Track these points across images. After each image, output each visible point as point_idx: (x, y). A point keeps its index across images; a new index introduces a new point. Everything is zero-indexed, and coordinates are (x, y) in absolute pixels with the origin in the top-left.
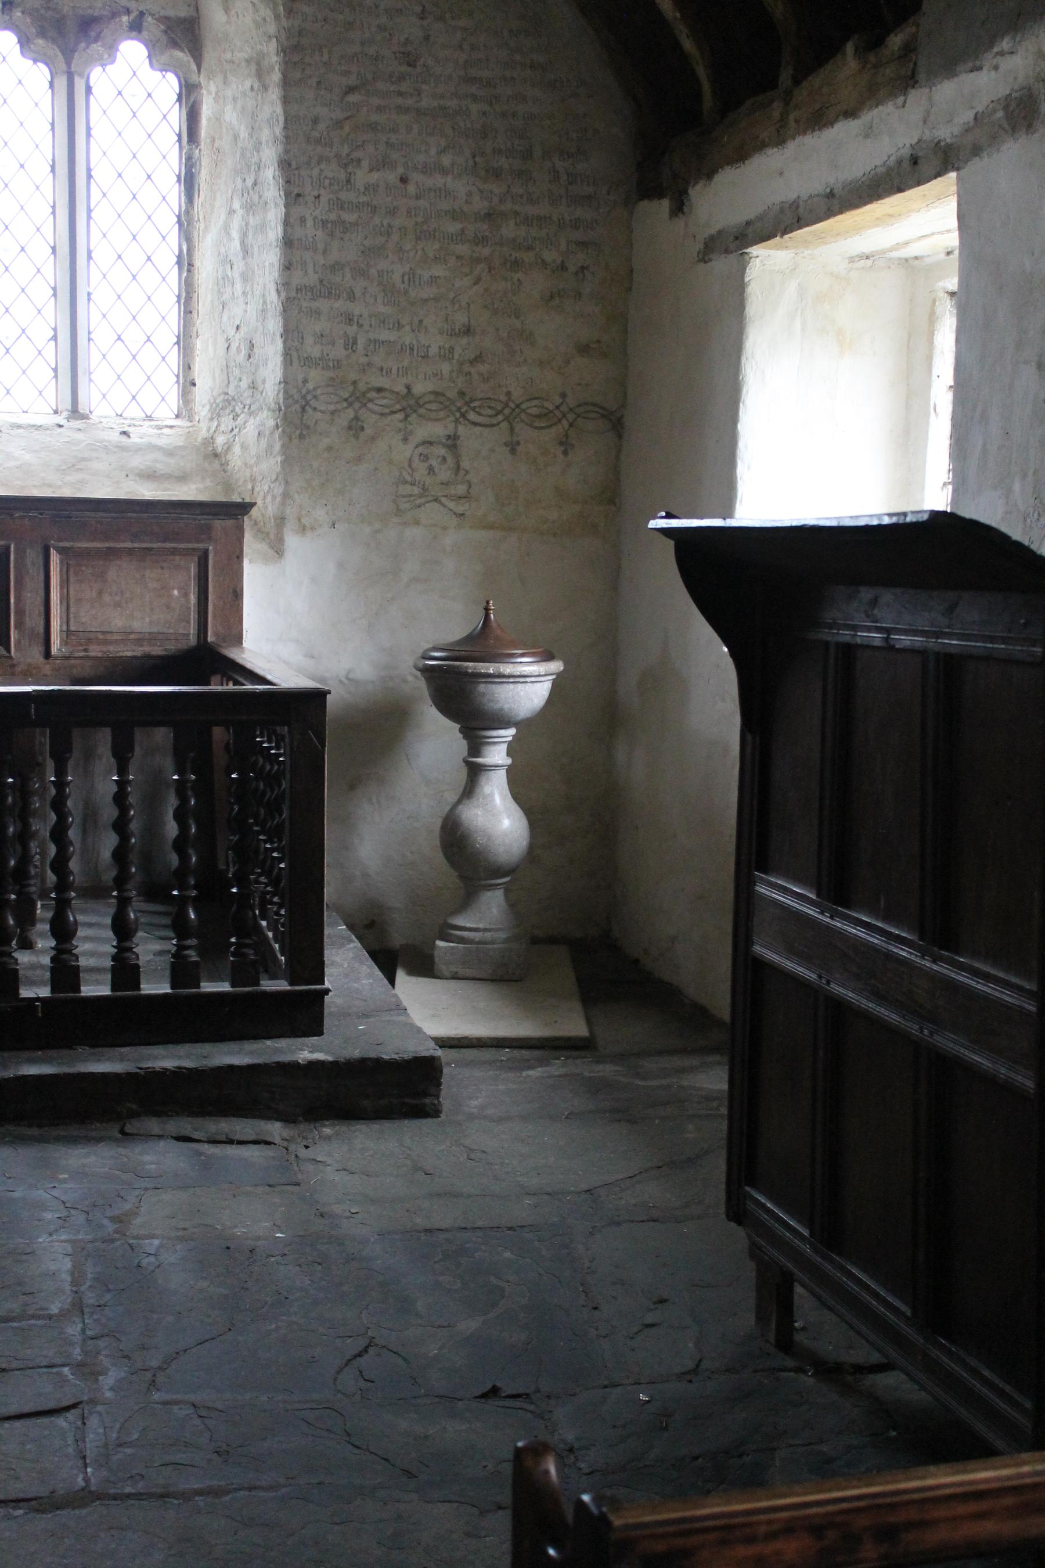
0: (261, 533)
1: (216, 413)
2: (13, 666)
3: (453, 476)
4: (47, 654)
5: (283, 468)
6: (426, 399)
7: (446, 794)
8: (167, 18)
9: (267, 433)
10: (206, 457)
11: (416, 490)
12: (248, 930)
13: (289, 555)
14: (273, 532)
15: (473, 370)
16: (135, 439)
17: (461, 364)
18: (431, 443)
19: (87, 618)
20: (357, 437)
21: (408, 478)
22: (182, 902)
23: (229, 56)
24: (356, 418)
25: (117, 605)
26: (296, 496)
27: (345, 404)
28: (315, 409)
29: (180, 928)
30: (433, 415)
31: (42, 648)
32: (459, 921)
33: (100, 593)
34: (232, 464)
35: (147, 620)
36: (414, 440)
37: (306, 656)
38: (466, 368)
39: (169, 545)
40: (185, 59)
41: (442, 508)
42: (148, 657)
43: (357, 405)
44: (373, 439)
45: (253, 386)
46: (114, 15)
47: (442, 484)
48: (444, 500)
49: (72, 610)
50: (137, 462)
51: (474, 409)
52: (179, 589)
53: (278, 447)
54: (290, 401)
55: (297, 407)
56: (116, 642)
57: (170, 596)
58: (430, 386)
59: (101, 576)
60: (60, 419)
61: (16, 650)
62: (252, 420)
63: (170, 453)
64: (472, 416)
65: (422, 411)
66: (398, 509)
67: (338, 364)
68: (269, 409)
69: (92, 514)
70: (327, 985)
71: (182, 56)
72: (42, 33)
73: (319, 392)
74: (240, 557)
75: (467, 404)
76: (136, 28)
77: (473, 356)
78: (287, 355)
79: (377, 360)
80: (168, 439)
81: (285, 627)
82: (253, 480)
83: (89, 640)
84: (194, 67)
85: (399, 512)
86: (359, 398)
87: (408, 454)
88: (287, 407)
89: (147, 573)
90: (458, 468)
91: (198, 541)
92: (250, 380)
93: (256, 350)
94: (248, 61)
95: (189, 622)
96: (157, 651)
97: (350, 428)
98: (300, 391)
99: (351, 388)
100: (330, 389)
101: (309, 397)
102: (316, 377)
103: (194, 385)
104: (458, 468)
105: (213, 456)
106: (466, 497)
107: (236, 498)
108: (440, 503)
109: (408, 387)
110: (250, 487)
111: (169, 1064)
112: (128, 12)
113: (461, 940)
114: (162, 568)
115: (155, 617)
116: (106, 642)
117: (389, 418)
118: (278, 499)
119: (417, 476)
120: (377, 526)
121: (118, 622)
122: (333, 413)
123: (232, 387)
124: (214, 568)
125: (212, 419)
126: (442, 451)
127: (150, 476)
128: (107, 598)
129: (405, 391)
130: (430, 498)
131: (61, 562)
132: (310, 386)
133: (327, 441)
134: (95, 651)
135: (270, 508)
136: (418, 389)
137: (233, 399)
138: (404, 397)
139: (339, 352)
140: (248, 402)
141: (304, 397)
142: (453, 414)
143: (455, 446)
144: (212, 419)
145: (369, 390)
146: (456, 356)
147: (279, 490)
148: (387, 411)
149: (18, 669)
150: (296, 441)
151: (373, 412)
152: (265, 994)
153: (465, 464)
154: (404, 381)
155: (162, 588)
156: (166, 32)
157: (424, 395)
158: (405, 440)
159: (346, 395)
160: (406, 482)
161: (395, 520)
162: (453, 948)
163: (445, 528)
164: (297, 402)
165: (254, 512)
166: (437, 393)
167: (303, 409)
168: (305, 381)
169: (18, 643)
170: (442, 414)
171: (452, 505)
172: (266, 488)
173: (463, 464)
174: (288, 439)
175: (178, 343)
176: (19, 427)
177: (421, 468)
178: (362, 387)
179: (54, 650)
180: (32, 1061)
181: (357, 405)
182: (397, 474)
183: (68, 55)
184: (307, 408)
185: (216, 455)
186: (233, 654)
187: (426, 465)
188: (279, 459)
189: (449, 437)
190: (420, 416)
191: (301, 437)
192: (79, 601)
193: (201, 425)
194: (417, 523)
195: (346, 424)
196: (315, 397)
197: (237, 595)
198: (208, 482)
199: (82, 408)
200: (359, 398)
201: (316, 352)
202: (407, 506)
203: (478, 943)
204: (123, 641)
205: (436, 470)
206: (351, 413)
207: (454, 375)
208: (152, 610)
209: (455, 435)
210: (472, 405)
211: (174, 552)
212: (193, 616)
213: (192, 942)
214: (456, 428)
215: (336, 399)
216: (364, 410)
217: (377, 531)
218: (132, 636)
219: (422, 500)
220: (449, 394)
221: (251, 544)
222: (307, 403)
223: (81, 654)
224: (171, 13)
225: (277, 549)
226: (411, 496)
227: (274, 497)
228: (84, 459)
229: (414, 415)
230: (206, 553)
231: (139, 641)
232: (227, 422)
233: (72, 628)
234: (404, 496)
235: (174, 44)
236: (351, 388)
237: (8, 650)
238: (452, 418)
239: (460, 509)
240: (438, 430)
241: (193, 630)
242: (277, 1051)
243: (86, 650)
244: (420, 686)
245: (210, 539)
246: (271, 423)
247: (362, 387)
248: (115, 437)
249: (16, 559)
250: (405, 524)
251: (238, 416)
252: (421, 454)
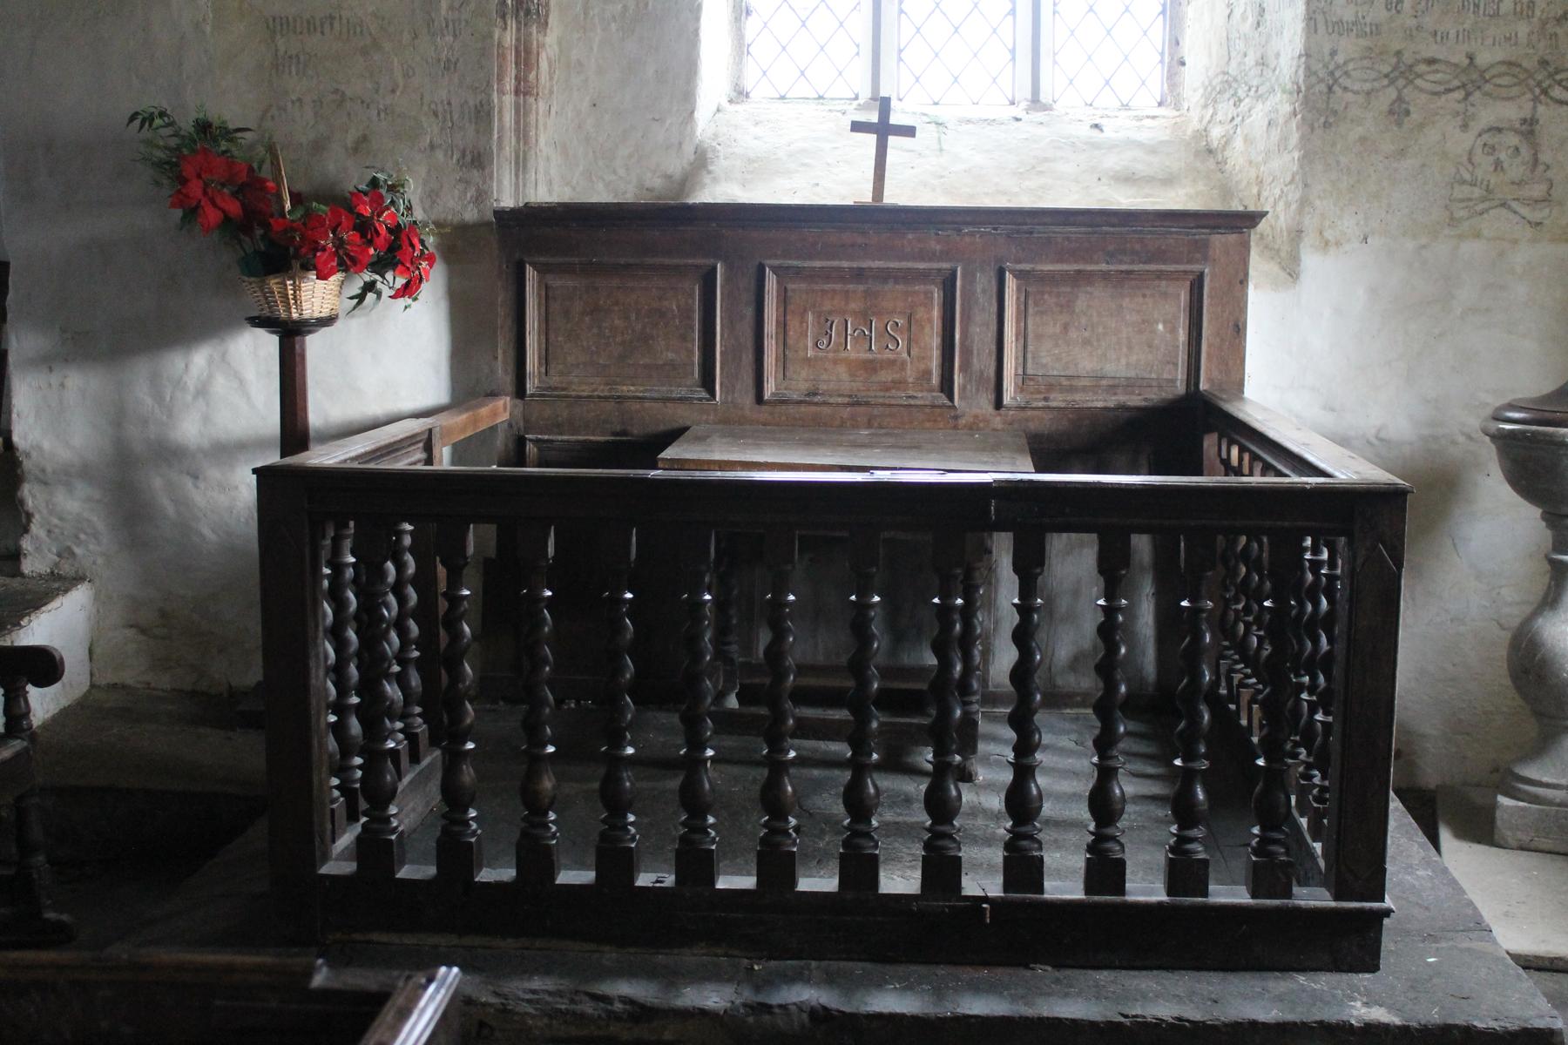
0: (1271, 251)
1: (1211, 99)
2: (956, 418)
4: (998, 404)
5: (1301, 167)
6: (1494, 71)
7: (1504, 591)
9: (1281, 121)
10: (1197, 154)
11: (1477, 192)
12: (1274, 818)
13: (1306, 278)
14: (1286, 248)
15: (1559, 31)
16: (1109, 133)
17: (1544, 23)
18: (1499, 130)
19: (1052, 359)
20: (1399, 124)
21: (1467, 176)
22: (1187, 777)
24: (1400, 99)
25: (1087, 342)
26: (1318, 203)
27: (1386, 82)
28: (1345, 89)
29: (1184, 812)
30: (1504, 92)
31: (992, 397)
32: (1530, 771)
33: (1066, 327)
34: (1231, 162)
35: (1123, 361)
36: (1476, 126)
37: (1324, 408)
38: (1550, 28)
39: (1153, 267)
41: (1511, 216)
42: (1124, 408)
43: (1401, 82)
44: (1421, 126)
45: (1262, 63)
48: (1515, 205)
49: (1030, 348)
50: (1112, 162)
51: (1559, 83)
52: (1165, 323)
53: (1295, 138)
54: (1313, 79)
55: (1323, 87)
56: (1084, 389)
57: (1154, 331)
58: (1500, 54)
59: (1068, 307)
60: (1018, 111)
61: (960, 398)
62: (1260, 106)
63: (1152, 150)
64: (1557, 92)
65: (1488, 87)
66: (1452, 219)
67: (1376, 29)
68: (1284, 91)
69: (1058, 229)
70: (1388, 902)
73: (1351, 66)
74: (1244, 282)
75: (1551, 76)
77: (1560, 12)
78: (1311, 20)
79: (1429, 21)
80: (1153, 132)
81: (1314, 377)
82: (1260, 182)
83: (1050, 387)
85: (1453, 221)
86: (1403, 72)
87: (1467, 145)
88: (1308, 88)
89: (1126, 302)
90: (1536, 162)
91: (1189, 262)
92: (1259, 55)
93: (1267, 16)
95: (1176, 365)
96: (1135, 401)
97: (1391, 112)
98: (1326, 66)
99: (1394, 60)
100: (1366, 63)
101: (1337, 74)
102: (1348, 47)
103: (1183, 64)
104: (1536, 162)
105: (1208, 153)
106: (1546, 200)
107: (1236, 206)
108: (1509, 208)
109: (1471, 58)
110: (1255, 190)
111: (1165, 1011)
113: (1535, 799)
114: (1144, 296)
115: (1134, 358)
116: (1072, 389)
117: (1443, 98)
118: (1294, 207)
119: (1479, 173)
120: (1424, 241)
121: (1086, 363)
122: (1368, 93)
123: (1234, 64)
124: (1211, 297)
125: (1205, 106)
126: (1513, 140)
127: (1127, 179)
128: (1073, 334)
129: (1467, 61)
130: (1497, 202)
131: (1019, 289)
132: (1340, 59)
133: (1360, 130)
134: (1058, 400)
135: (1282, 218)
136: (1484, 58)
137: (1235, 80)
138: (1464, 71)
139: (1378, 13)
140: (1255, 83)
141: (1332, 73)
142: (1531, 90)
143: (1532, 132)
144: (1205, 106)
145: (1418, 62)
146: (1538, 13)
147: (1294, 195)
148: (1441, 88)
149: (962, 422)
150: (1319, 132)
151: (1422, 90)
152: (1298, 909)
153: (1545, 157)
154: (1466, 48)
155: (1144, 322)
157: (1492, 66)
158: (1465, 127)
159: (1386, 69)
160: (1464, 182)
161: (1447, 231)
162: (1522, 809)
163: (1515, 242)
164: (1321, 81)
165: (1263, 226)
166: (1510, 64)
167: (1330, 88)
168: (1333, 53)
169: (963, 389)
170: (1515, 91)
171: (1525, 211)
172: (1277, 192)
173: (1543, 157)
174: (1309, 127)
175: (1163, 12)
176: (969, 121)
177: (1485, 163)
178: (1408, 58)
179: (1007, 399)
180: (976, 988)
181: (1401, 82)
182: (1453, 170)
184: (1336, 88)
185: (1210, 151)
186: (1233, 408)
187: (1491, 158)
188: (1296, 155)
189: (1524, 121)
191: (1327, 125)
192: (1039, 337)
193: (1192, 113)
194: (1478, 235)
195: (1385, 108)
196: (1346, 73)
197: (1239, 330)
198: (1201, 187)
199: (1044, 97)
200: (1403, 72)
201: (1348, 15)
202: (1462, 213)
203: (1559, 805)
204: (1094, 388)
205: (1505, 165)
206: (1392, 93)
207: (1534, 38)
208: (1130, 348)
210: (1558, 77)
211: (1160, 275)
212: (1182, 358)
213: (1197, 832)
214: (1535, 108)
215: (1373, 75)
216: (1410, 88)
217: (1424, 247)
218: (1104, 382)
219: (1487, 205)
220: (1525, 64)
221: (1259, 266)
222: (1336, 81)
223: (1040, 404)
225: (1291, 270)
226: (1470, 199)
227: (1288, 205)
228: (1046, 160)
229: (1477, 94)
230: (1201, 276)
231: (1112, 389)
232: (1225, 109)
233: (1030, 371)
234: (1462, 201)
236: (1394, 60)
237: (951, 398)
238: (1529, 96)
239: (1536, 216)
240: (1511, 112)
241: (1181, 375)
242: (1316, 997)
243: (1046, 399)
244: (1489, 454)
245: (1205, 259)
246: (1287, 108)
247: (1408, 58)
248: (1085, 131)
249: (963, 286)
250: (1461, 237)
251: (1240, 101)
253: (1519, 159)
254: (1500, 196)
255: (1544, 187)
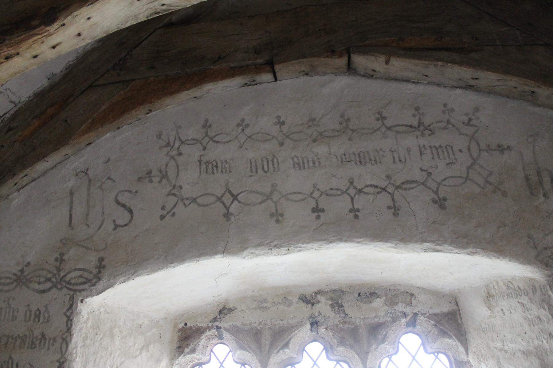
8: (435, 315)
23: (499, 345)
40: (454, 343)
46: (395, 320)
71: (452, 342)
72: (342, 342)
76: (412, 324)
84: (462, 349)
94: (526, 354)
112: (405, 315)
156: (436, 325)
183: (364, 356)
224: (437, 310)
235: (444, 333)
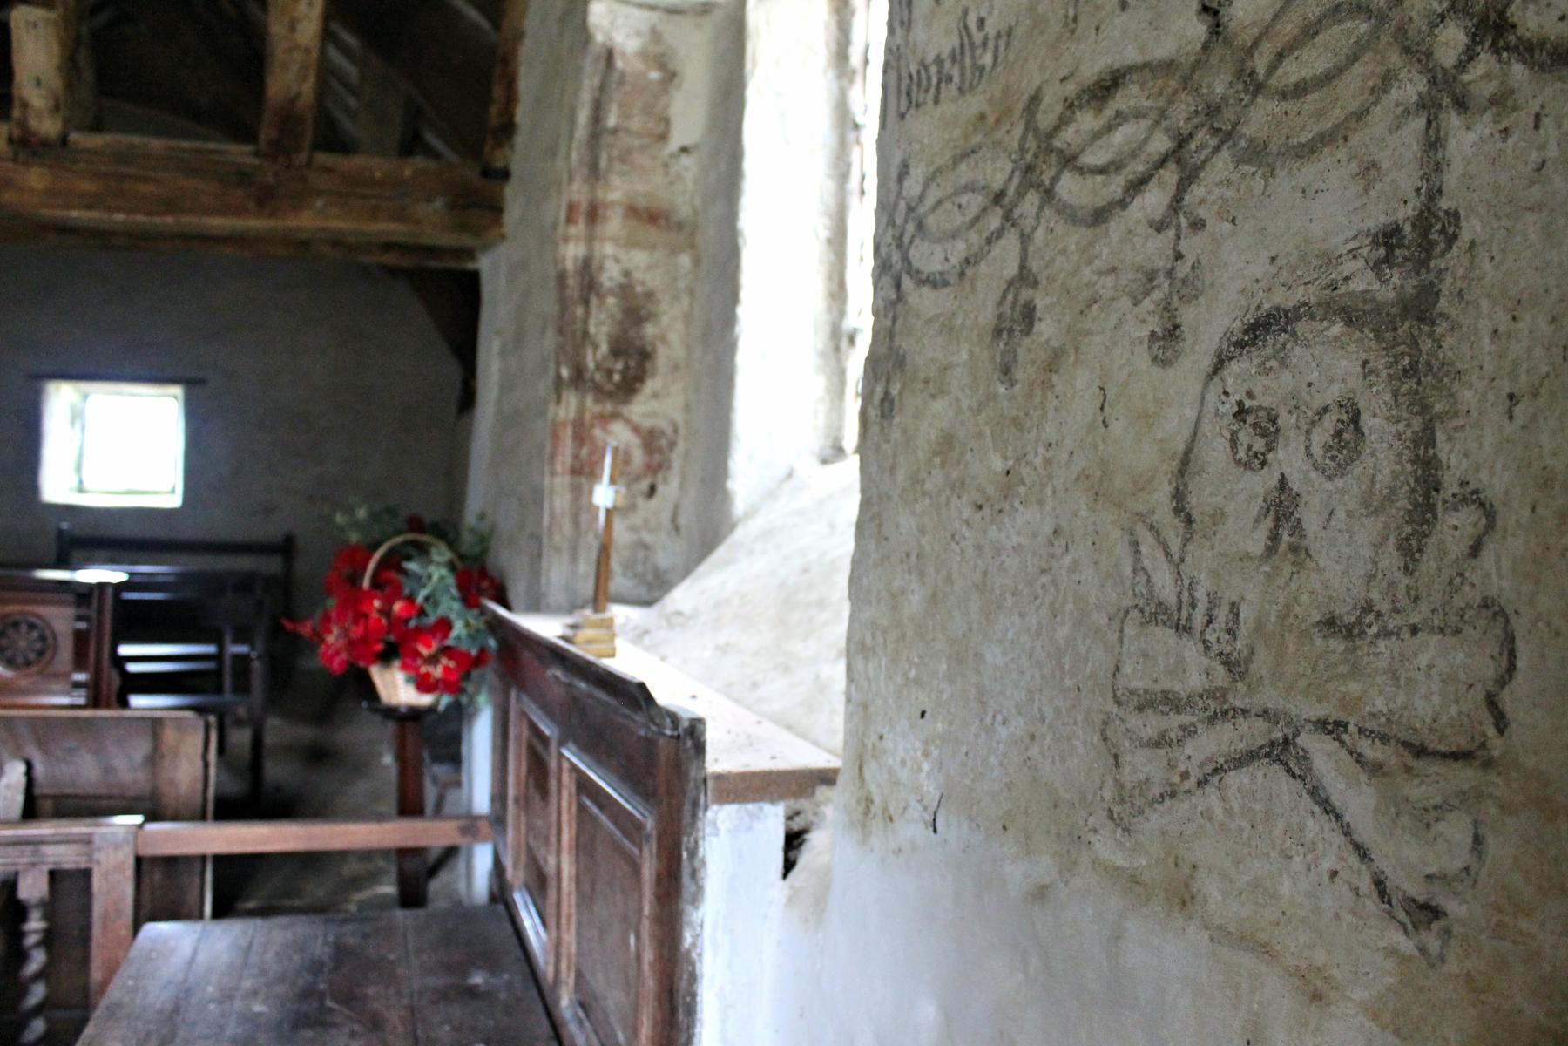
3: (1391, 559)
41: (1316, 826)
47: (1330, 624)
87: (1174, 426)
108: (1300, 770)
130: (1254, 732)
143: (1421, 307)
190: (1256, 154)
209: (1423, 221)
214: (1433, 143)
234: (1147, 703)
238: (1411, 87)
252: (1241, 412)
253: (1351, 485)
254: (1270, 697)
255: (1471, 659)
